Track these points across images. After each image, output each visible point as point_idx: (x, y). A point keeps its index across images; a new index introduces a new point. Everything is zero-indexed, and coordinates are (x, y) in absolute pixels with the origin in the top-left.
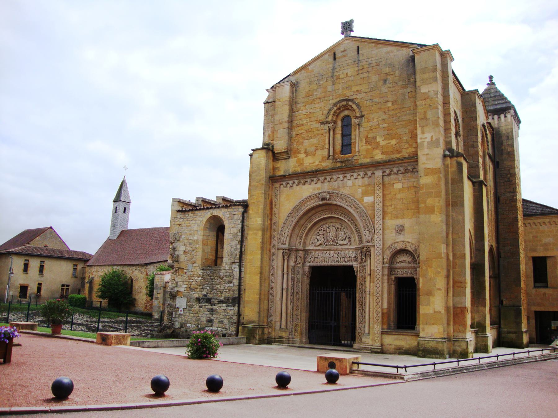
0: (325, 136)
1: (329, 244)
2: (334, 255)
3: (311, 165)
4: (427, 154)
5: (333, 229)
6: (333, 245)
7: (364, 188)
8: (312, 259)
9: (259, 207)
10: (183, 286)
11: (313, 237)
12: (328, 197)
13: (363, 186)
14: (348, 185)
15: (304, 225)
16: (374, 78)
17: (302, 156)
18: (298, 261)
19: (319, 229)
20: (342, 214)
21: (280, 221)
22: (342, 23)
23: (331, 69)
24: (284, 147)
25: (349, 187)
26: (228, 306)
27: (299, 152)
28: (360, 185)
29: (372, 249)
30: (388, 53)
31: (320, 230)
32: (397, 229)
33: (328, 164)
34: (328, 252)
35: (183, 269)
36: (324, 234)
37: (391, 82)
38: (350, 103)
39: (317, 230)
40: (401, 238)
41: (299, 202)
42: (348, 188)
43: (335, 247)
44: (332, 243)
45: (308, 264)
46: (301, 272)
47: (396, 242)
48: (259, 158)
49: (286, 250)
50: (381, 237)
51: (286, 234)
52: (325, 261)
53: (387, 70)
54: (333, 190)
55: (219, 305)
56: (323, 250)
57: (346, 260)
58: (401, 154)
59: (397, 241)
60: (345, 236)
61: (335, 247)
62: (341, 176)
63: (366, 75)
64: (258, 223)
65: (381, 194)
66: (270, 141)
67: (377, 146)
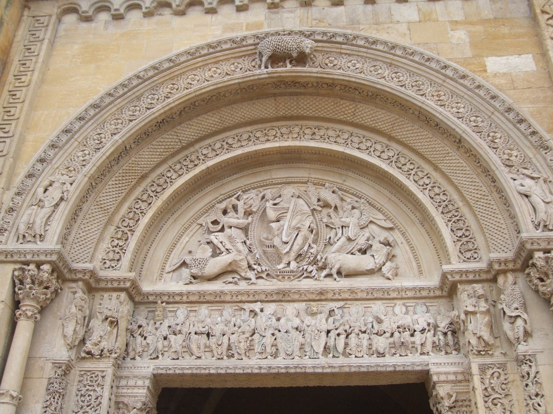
1: (280, 266)
2: (308, 320)
5: (296, 205)
7: (479, 28)
8: (176, 341)
11: (185, 239)
12: (308, 45)
13: (472, 24)
14: (396, 17)
15: (153, 176)
18: (95, 338)
19: (223, 206)
20: (356, 140)
21: (30, 137)
25: (405, 26)
31: (225, 212)
34: (270, 308)
36: (245, 230)
39: (211, 207)
41: (152, 63)
42: (403, 28)
43: (306, 284)
44: (293, 265)
46: (105, 402)
49: (38, 265)
51: (55, 194)
52: (250, 349)
57: (381, 343)
60: (367, 235)
61: (306, 284)
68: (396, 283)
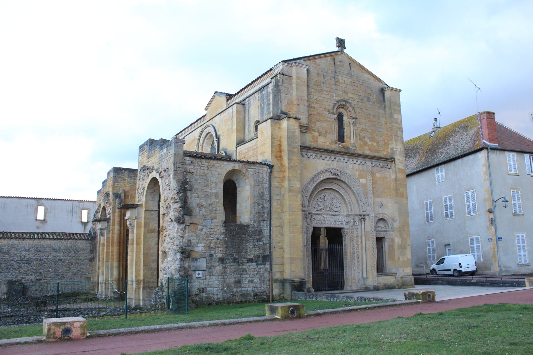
0: (332, 124)
3: (323, 144)
4: (399, 159)
6: (329, 211)
7: (360, 172)
9: (297, 172)
10: (199, 245)
12: (339, 174)
16: (362, 94)
17: (316, 134)
22: (344, 40)
23: (333, 71)
24: (305, 122)
26: (257, 265)
27: (314, 130)
28: (357, 169)
29: (367, 217)
30: (368, 79)
32: (380, 205)
33: (335, 147)
35: (196, 226)
37: (372, 101)
38: (348, 105)
40: (381, 211)
43: (330, 213)
45: (313, 226)
47: (379, 214)
48: (293, 126)
50: (373, 209)
53: (369, 92)
54: (341, 168)
55: (248, 264)
56: (322, 215)
58: (379, 154)
59: (380, 212)
61: (330, 213)
62: (346, 160)
63: (357, 88)
64: (298, 186)
65: (371, 179)
66: (287, 111)
67: (366, 144)
68: (340, 214)
